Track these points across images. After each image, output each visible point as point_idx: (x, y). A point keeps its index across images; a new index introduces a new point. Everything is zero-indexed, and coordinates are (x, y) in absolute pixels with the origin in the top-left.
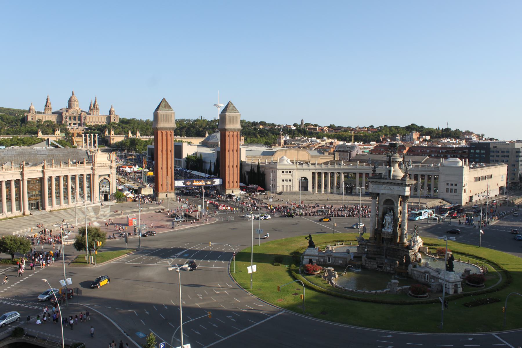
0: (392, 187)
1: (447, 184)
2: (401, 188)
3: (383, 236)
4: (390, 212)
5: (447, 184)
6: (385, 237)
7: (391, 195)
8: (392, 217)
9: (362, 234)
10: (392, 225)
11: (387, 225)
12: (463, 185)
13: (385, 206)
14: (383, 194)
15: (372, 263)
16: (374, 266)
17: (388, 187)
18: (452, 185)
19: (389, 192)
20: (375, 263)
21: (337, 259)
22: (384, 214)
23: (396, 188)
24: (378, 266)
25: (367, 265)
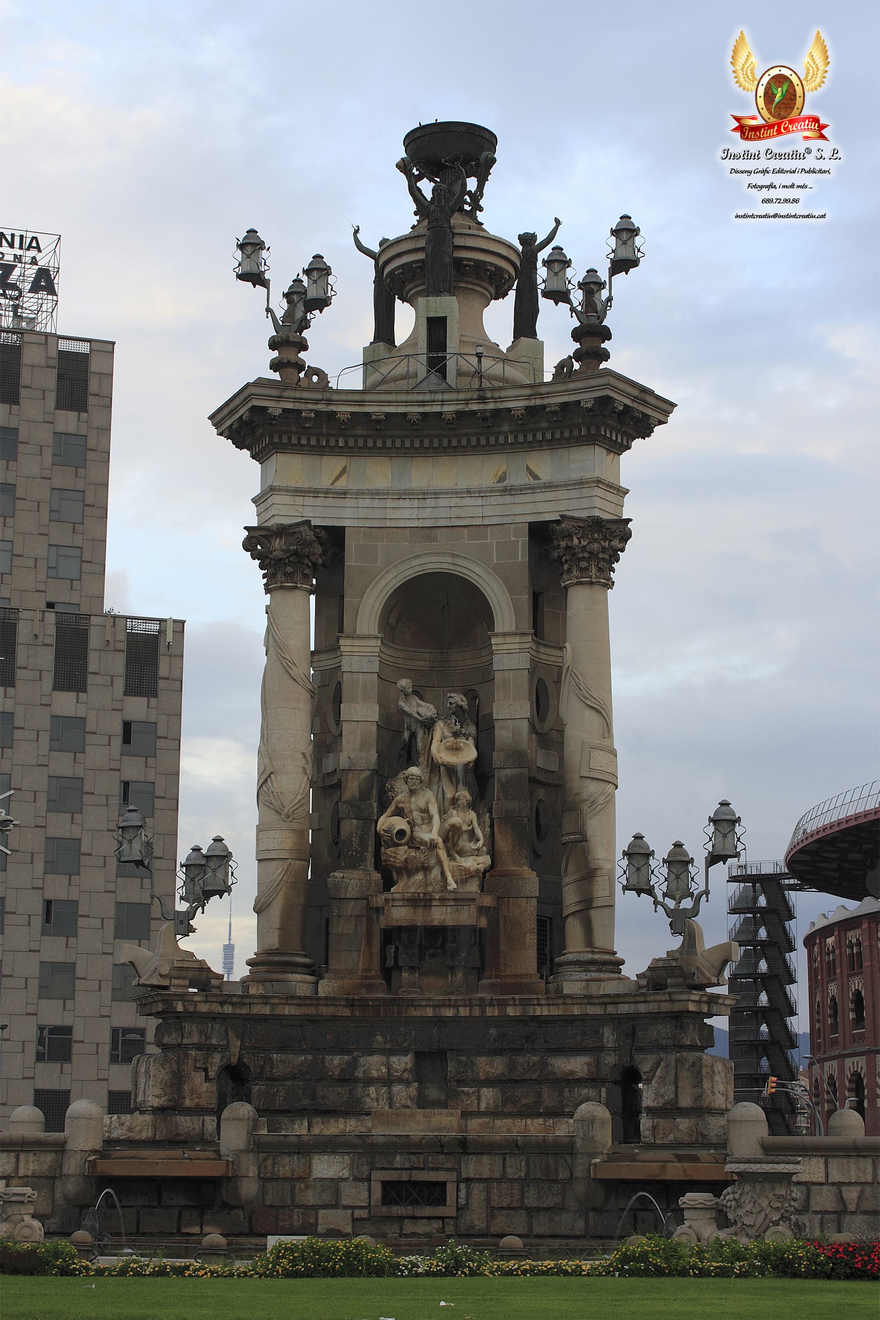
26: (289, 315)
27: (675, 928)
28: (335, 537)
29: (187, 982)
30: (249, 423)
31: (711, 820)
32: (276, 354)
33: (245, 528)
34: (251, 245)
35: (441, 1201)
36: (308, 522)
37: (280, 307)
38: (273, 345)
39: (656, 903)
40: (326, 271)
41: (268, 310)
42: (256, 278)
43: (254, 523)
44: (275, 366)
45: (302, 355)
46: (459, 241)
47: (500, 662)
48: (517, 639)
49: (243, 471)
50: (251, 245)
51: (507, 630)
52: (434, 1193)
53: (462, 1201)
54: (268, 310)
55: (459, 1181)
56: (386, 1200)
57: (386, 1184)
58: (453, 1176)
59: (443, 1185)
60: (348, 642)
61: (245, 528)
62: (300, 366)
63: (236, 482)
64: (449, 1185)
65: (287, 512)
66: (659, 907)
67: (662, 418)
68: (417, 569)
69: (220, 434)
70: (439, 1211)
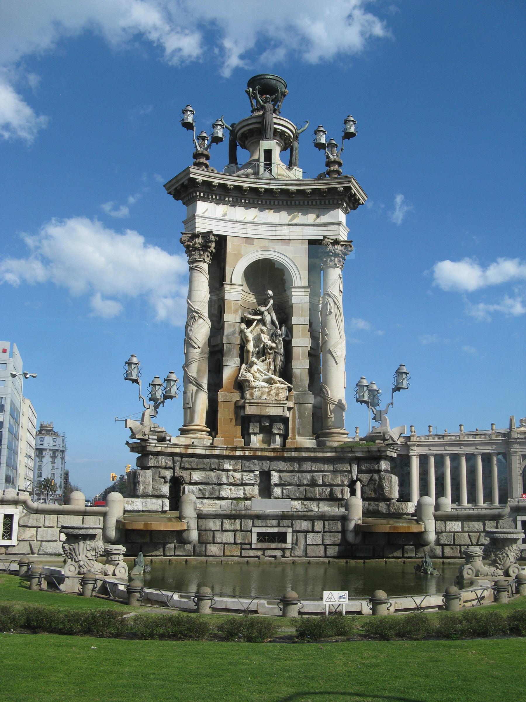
28: (222, 240)
35: (285, 542)
46: (275, 121)
47: (294, 300)
48: (303, 290)
51: (299, 285)
52: (281, 538)
55: (293, 531)
56: (259, 540)
57: (259, 534)
58: (290, 530)
59: (285, 534)
64: (288, 534)
65: (201, 226)
68: (260, 256)
69: (170, 193)
70: (283, 545)
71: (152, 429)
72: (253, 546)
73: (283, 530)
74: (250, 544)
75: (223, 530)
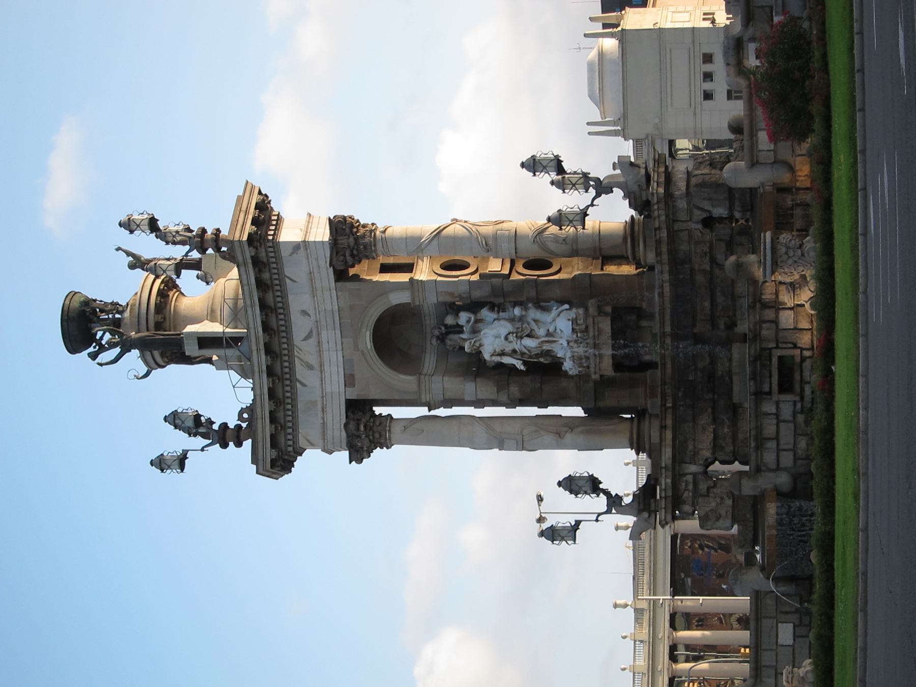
0: (300, 326)
1: (708, 96)
2: (295, 272)
3: (607, 368)
4: (459, 329)
5: (708, 96)
6: (608, 352)
7: (348, 329)
8: (485, 313)
9: (614, 502)
10: (533, 313)
11: (530, 343)
12: (707, 24)
13: (429, 362)
14: (349, 380)
15: (770, 429)
16: (787, 411)
17: (304, 350)
18: (708, 76)
19: (331, 337)
20: (768, 407)
21: (767, 658)
22: (476, 367)
23: (299, 301)
24: (785, 386)
25: (787, 460)
26: (205, 436)
27: (609, 190)
29: (652, 501)
30: (278, 460)
31: (535, 175)
32: (231, 444)
33: (350, 462)
34: (160, 463)
36: (346, 425)
37: (200, 442)
38: (224, 446)
39: (592, 205)
40: (175, 414)
41: (202, 450)
42: (181, 461)
43: (346, 454)
44: (239, 444)
45: (231, 426)
49: (311, 461)
50: (160, 463)
53: (791, 346)
54: (202, 450)
55: (777, 347)
58: (774, 351)
60: (423, 397)
61: (350, 462)
62: (239, 427)
63: (320, 467)
66: (595, 203)
67: (257, 191)
71: (642, 507)
72: (798, 398)
73: (775, 361)
74: (795, 402)
75: (777, 438)
